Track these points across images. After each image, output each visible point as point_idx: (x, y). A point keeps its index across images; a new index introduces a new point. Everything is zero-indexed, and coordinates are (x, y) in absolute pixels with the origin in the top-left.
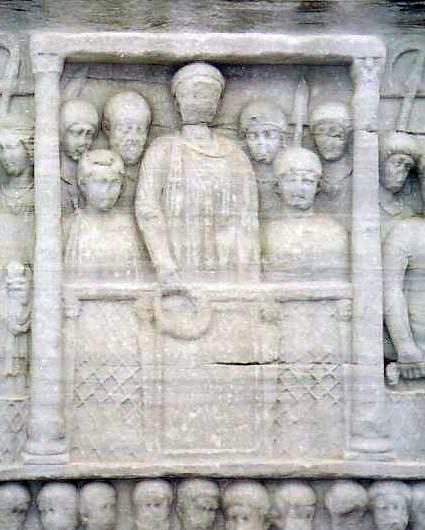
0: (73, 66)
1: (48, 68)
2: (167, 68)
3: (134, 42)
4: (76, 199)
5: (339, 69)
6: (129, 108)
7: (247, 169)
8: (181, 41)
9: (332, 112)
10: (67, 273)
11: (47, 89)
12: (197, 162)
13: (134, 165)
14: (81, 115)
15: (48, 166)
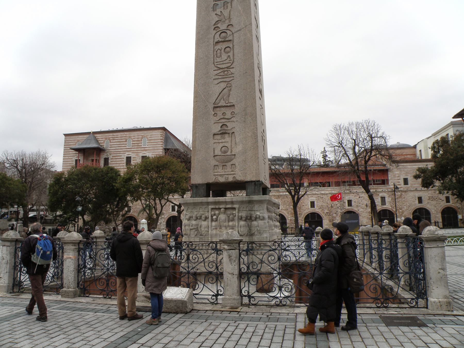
0: (212, 209)
1: (210, 209)
2: (220, 209)
3: (217, 207)
4: (212, 220)
5: (234, 209)
6: (217, 212)
7: (227, 218)
8: (221, 207)
9: (234, 212)
10: (211, 227)
11: (210, 211)
12: (222, 217)
13: (217, 217)
14: (213, 213)
15: (210, 218)
